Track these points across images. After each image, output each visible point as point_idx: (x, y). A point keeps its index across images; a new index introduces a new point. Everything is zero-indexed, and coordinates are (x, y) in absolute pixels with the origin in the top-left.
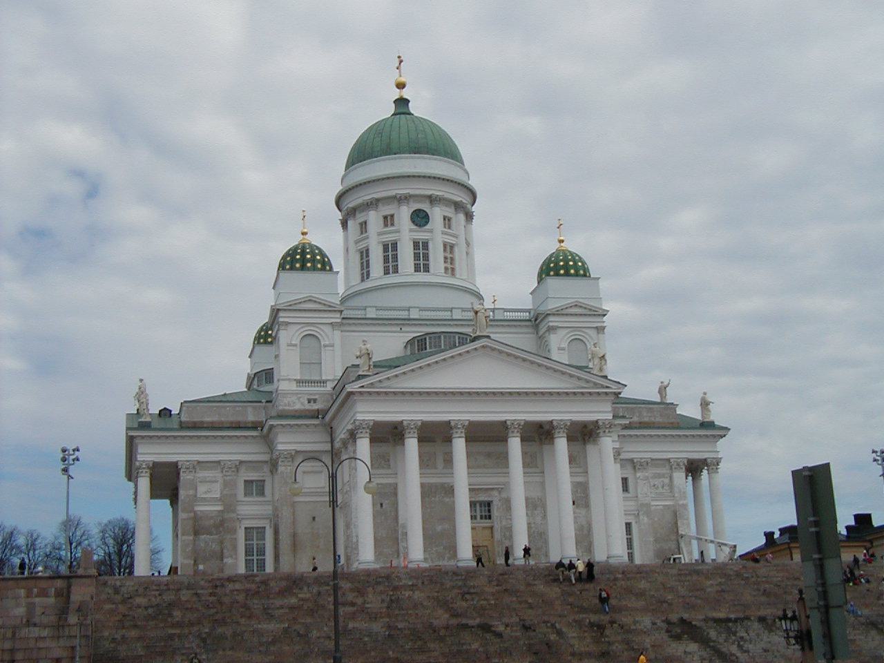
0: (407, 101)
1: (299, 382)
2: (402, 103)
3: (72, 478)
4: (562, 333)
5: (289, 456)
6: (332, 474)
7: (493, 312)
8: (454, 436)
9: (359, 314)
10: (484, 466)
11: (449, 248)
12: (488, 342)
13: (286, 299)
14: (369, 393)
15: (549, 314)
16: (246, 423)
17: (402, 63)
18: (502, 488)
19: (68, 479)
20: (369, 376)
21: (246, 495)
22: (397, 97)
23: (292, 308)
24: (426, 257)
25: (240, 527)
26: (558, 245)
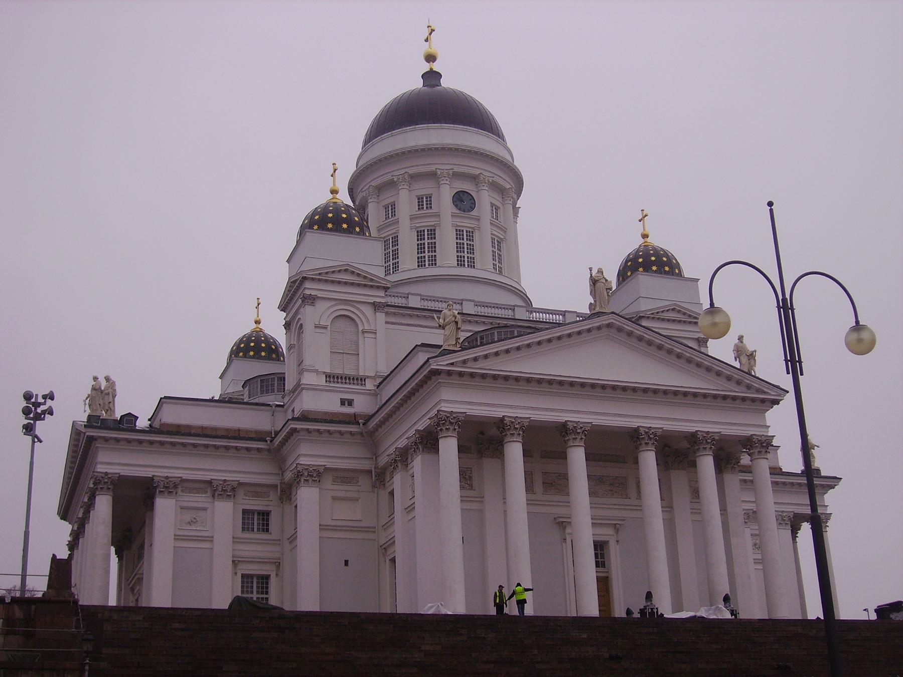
0: (438, 75)
1: (330, 377)
2: (432, 77)
3: (41, 442)
6: (784, 300)
7: (564, 315)
9: (401, 302)
12: (615, 320)
13: (310, 266)
14: (461, 374)
15: (643, 317)
16: (247, 431)
17: (433, 33)
18: (620, 525)
19: (34, 442)
20: (455, 352)
22: (428, 70)
23: (324, 277)
24: (471, 250)
25: (236, 573)
26: (641, 241)
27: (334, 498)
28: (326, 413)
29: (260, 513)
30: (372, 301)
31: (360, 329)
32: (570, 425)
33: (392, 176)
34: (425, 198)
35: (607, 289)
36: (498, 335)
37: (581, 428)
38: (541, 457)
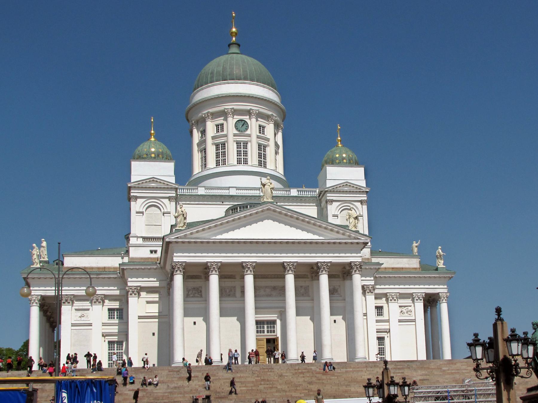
1: (145, 238)
4: (335, 204)
5: (135, 291)
8: (245, 273)
10: (270, 296)
11: (262, 148)
14: (183, 242)
15: (327, 191)
21: (109, 318)
24: (246, 153)
27: (148, 302)
28: (142, 258)
29: (117, 309)
30: (168, 196)
31: (162, 211)
32: (244, 264)
33: (202, 114)
34: (220, 126)
35: (271, 189)
36: (240, 209)
37: (251, 265)
38: (240, 279)
